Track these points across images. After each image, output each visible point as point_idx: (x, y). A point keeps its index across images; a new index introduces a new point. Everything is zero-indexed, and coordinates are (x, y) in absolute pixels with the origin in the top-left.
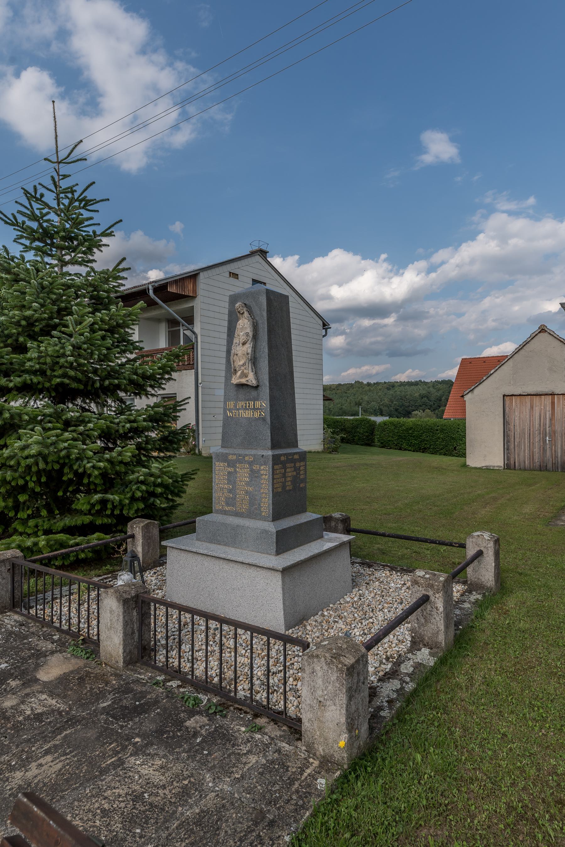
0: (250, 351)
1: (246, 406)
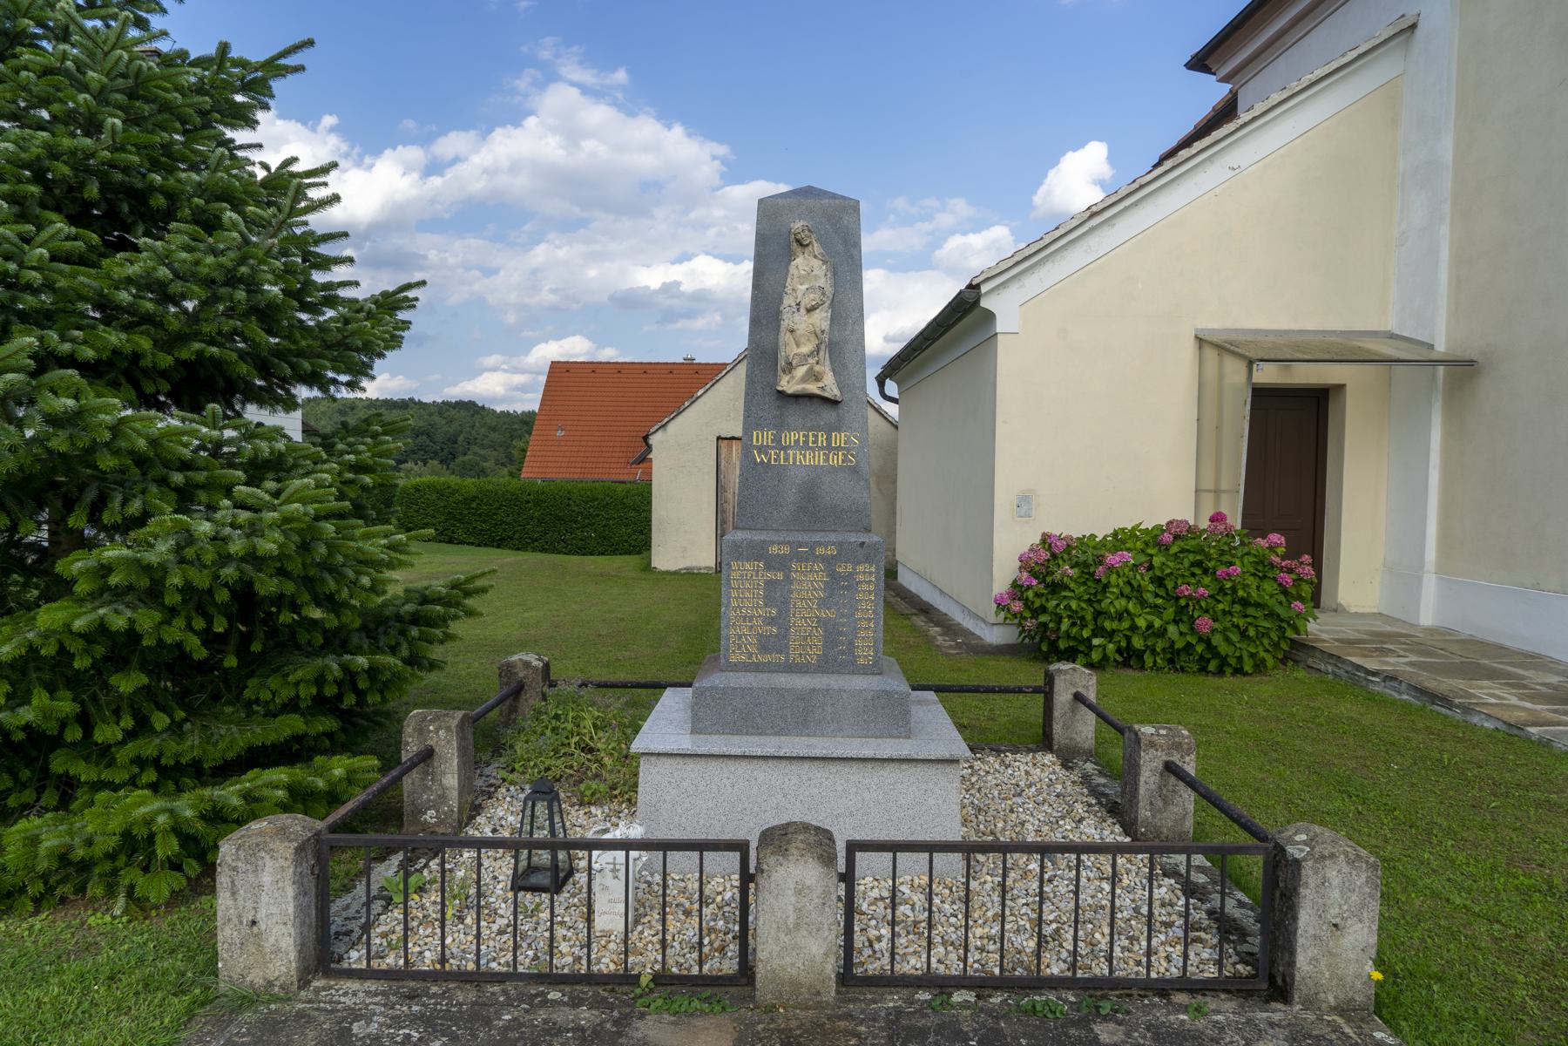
0: (825, 325)
1: (806, 442)
